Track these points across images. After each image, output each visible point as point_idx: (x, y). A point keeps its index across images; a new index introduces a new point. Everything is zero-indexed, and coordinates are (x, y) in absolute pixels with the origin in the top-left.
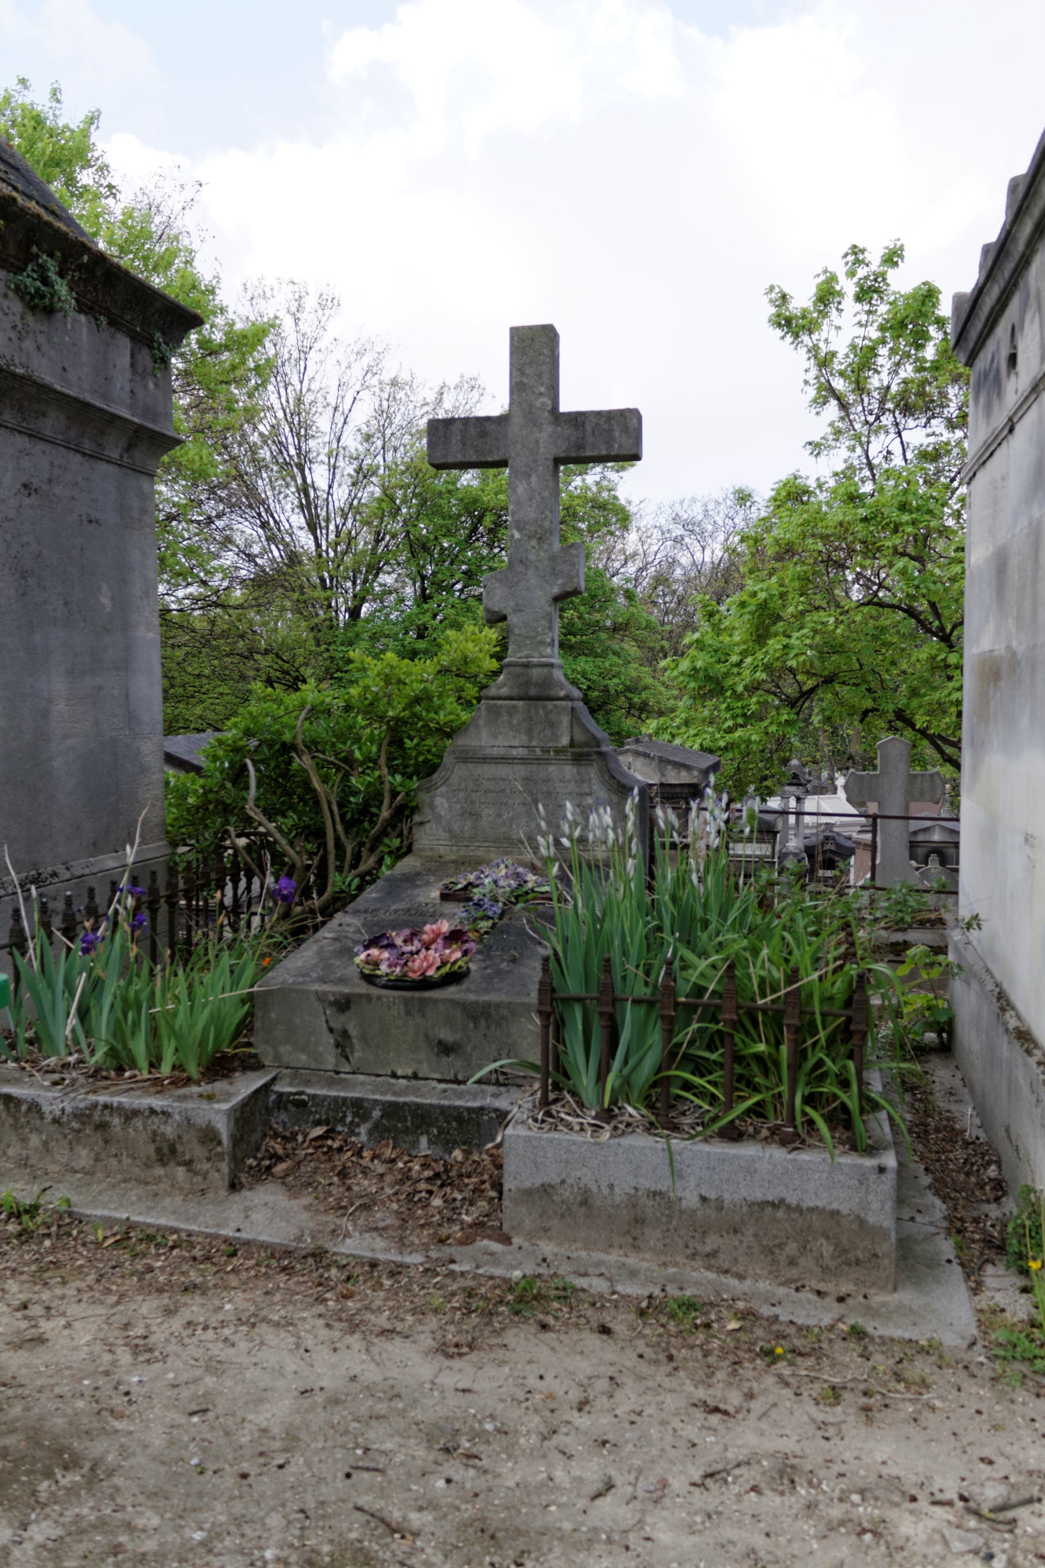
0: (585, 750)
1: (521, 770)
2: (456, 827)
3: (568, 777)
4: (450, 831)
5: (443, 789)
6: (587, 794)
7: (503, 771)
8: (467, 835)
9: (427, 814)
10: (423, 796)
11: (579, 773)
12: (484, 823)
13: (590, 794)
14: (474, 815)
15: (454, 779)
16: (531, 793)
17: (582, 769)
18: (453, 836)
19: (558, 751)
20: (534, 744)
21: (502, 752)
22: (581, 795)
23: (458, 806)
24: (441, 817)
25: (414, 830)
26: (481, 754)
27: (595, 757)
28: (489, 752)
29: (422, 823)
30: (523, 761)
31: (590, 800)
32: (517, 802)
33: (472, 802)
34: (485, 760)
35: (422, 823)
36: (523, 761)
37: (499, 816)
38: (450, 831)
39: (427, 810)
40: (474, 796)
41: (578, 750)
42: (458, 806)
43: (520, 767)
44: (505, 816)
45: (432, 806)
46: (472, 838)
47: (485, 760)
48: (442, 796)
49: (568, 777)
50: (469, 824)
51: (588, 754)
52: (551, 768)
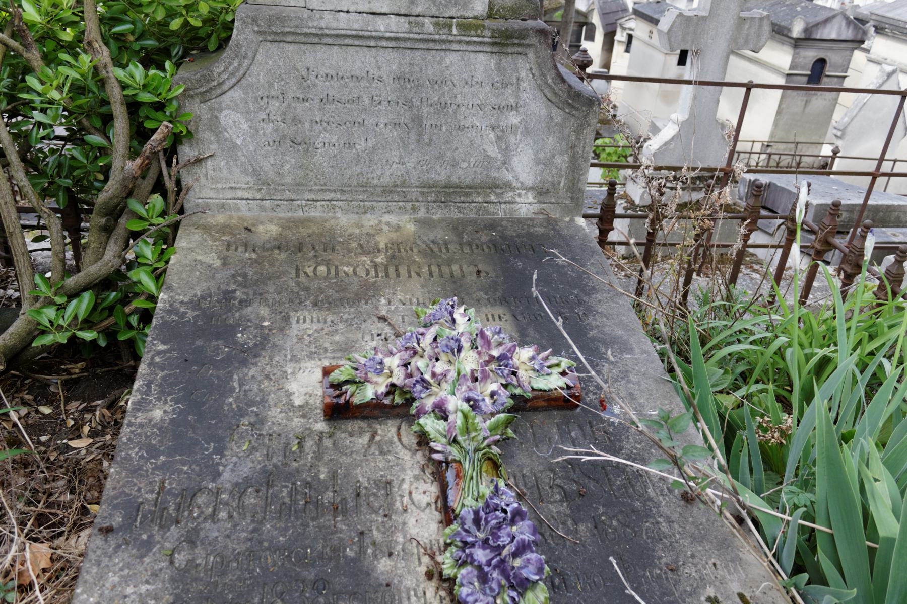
0: (516, 24)
1: (389, 63)
2: (266, 166)
3: (479, 76)
4: (256, 173)
5: (236, 94)
6: (511, 108)
7: (358, 61)
8: (288, 179)
9: (208, 143)
10: (196, 109)
11: (499, 68)
12: (321, 158)
13: (516, 108)
14: (301, 144)
15: (258, 74)
16: (408, 103)
17: (507, 61)
18: (262, 182)
19: (466, 27)
20: (419, 9)
21: (355, 23)
22: (499, 109)
23: (269, 128)
24: (235, 146)
25: (184, 173)
26: (312, 26)
27: (533, 40)
28: (329, 22)
29: (199, 161)
30: (397, 42)
31: (514, 119)
32: (383, 120)
33: (296, 121)
34: (319, 38)
35: (199, 161)
36: (397, 42)
37: (350, 145)
38: (256, 173)
39: (205, 135)
40: (300, 108)
41: (500, 24)
42: (269, 128)
43: (391, 55)
44: (361, 146)
45: (214, 126)
46: (298, 186)
47: (319, 38)
48: (235, 108)
49: (479, 76)
50: (291, 159)
51: (522, 34)
52: (450, 59)
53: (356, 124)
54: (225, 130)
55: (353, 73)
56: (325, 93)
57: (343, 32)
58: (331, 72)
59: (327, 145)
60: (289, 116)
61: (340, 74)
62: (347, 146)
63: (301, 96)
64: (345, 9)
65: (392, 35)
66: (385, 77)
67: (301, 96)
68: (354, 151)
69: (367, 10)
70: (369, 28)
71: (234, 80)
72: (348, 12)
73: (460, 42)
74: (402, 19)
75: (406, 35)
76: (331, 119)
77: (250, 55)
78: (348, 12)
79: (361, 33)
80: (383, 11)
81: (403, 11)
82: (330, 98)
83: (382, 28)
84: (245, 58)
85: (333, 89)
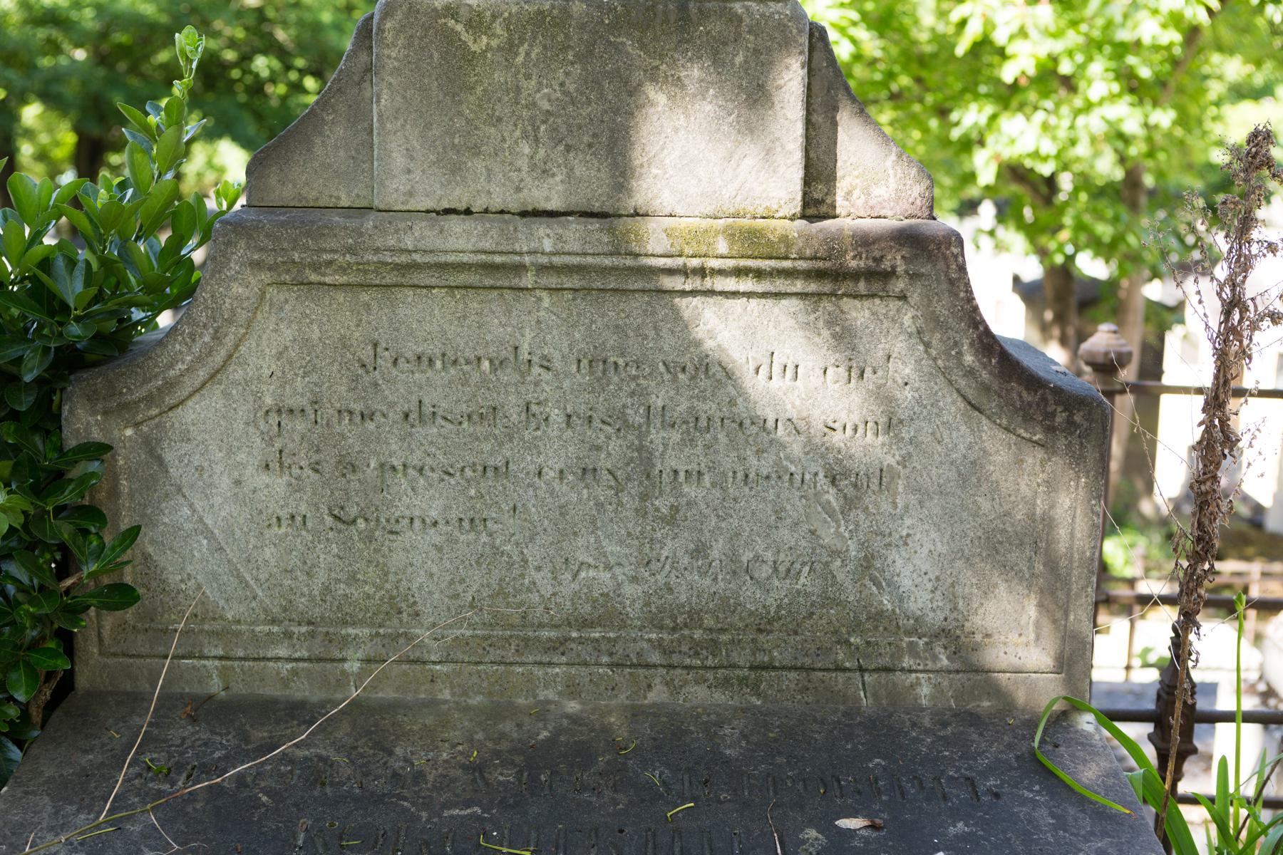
32: (552, 466)
53: (490, 473)
54: (179, 490)
55: (480, 352)
56: (414, 399)
57: (451, 258)
58: (433, 349)
59: (417, 523)
60: (329, 457)
61: (450, 354)
62: (466, 524)
63: (357, 407)
64: (462, 206)
65: (576, 260)
66: (556, 356)
67: (357, 407)
68: (484, 538)
69: (514, 206)
70: (517, 248)
71: (202, 374)
72: (468, 212)
73: (739, 272)
74: (595, 224)
75: (607, 262)
76: (429, 461)
77: (243, 316)
78: (468, 212)
79: (498, 259)
80: (553, 205)
81: (596, 206)
82: (428, 410)
83: (548, 245)
84: (230, 321)
85: (437, 389)
